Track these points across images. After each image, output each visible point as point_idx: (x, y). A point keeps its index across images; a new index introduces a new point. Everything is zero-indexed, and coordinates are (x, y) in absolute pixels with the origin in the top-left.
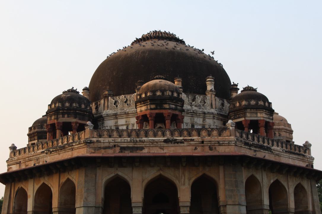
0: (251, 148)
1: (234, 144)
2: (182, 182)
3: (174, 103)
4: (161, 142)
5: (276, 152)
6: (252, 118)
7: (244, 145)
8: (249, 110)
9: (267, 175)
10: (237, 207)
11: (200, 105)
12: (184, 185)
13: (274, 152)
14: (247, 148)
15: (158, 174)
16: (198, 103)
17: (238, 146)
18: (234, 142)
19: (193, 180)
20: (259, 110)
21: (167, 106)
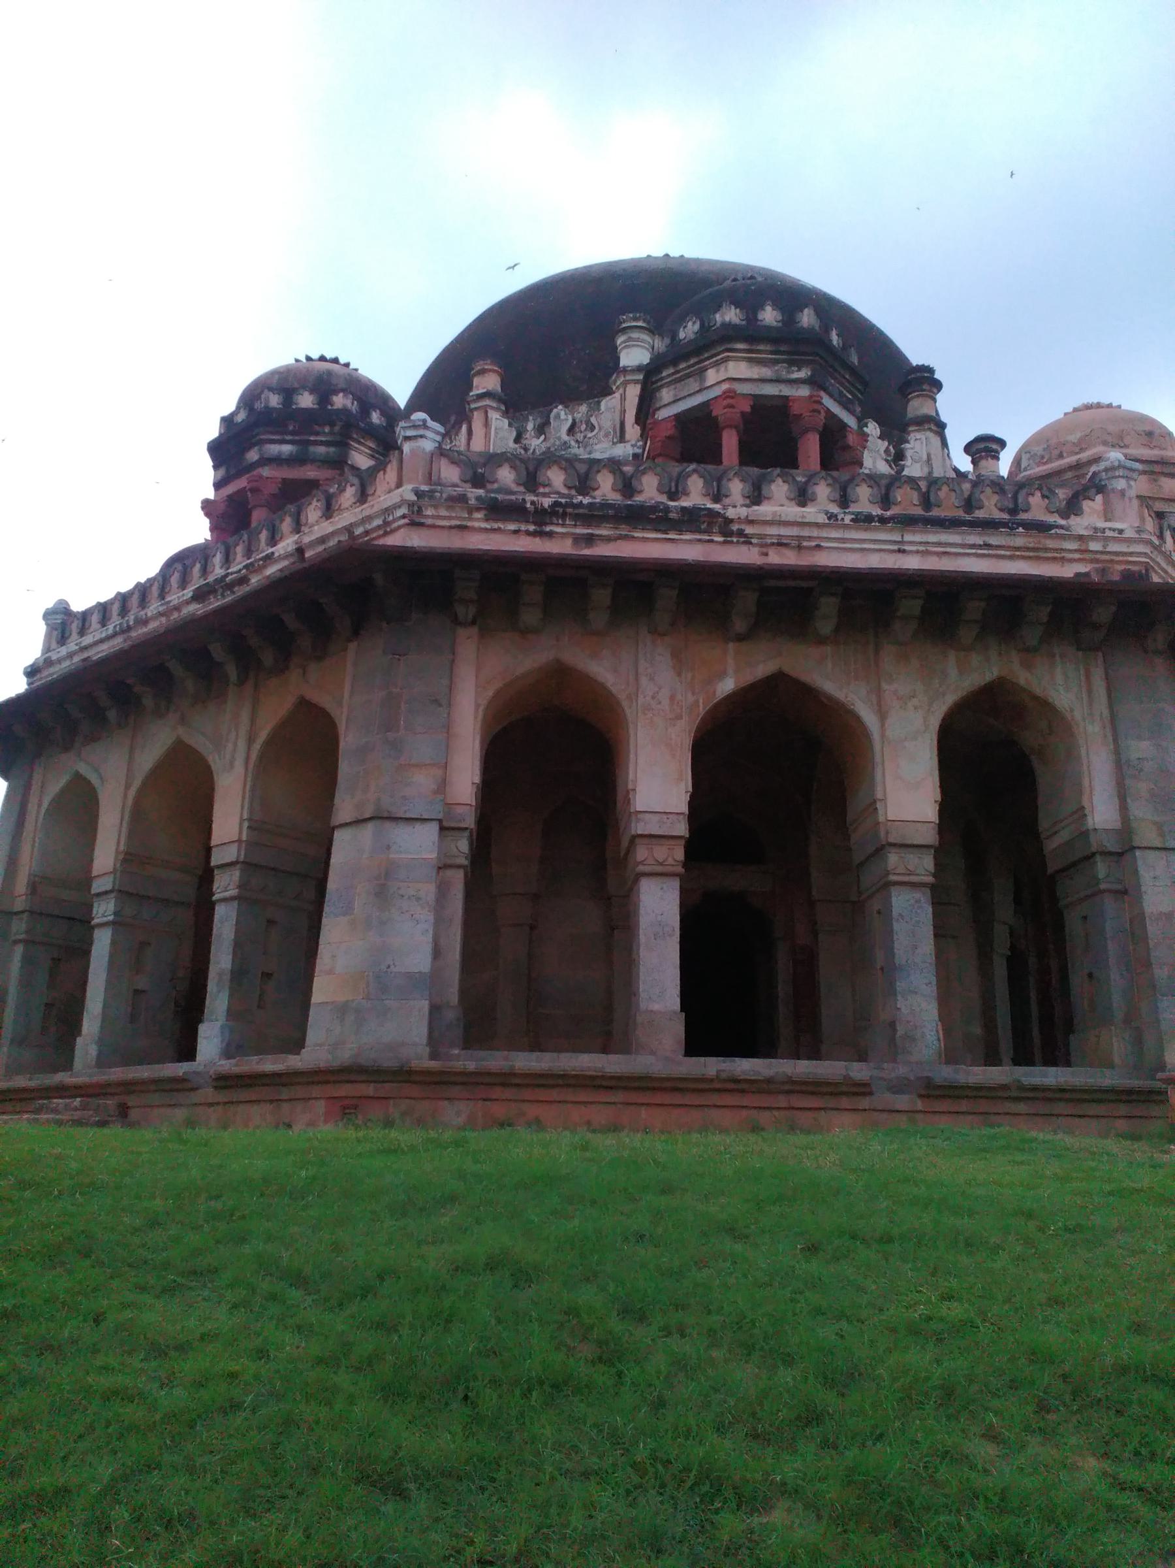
0: (548, 529)
1: (406, 521)
2: (228, 757)
3: (293, 433)
4: (188, 602)
5: (773, 531)
6: (680, 403)
7: (487, 520)
8: (671, 370)
9: (676, 655)
10: (369, 830)
11: (565, 443)
12: (232, 765)
13: (749, 530)
14: (516, 532)
15: (169, 742)
16: (559, 438)
17: (433, 526)
18: (404, 510)
19: (263, 736)
20: (714, 352)
21: (253, 456)
